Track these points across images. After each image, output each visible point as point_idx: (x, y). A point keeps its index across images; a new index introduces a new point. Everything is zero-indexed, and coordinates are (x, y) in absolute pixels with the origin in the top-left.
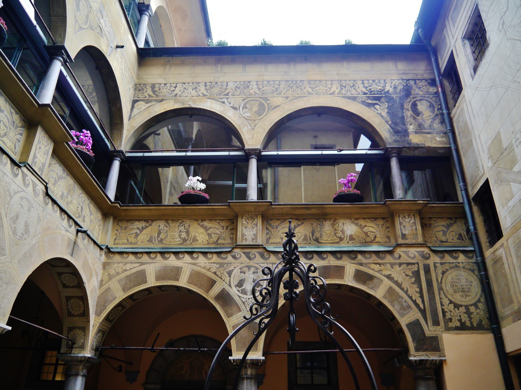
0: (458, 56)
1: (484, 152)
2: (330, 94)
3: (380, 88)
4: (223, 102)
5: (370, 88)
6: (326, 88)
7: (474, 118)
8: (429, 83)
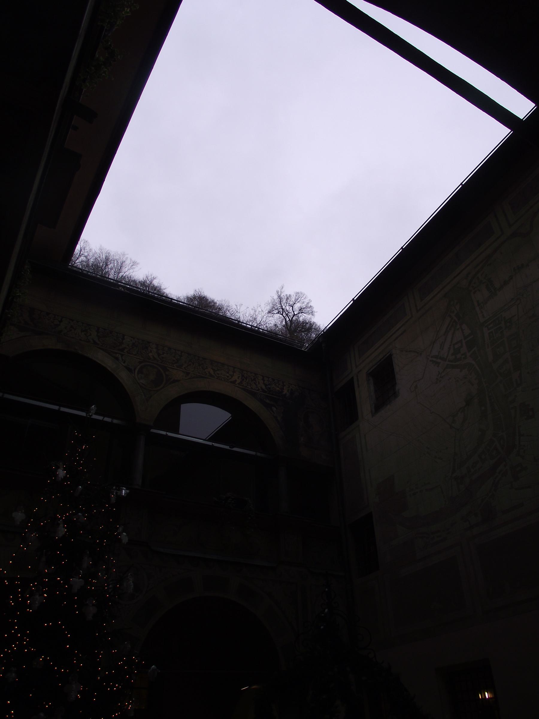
2: (231, 382)
3: (278, 389)
4: (117, 359)
5: (269, 386)
6: (228, 375)
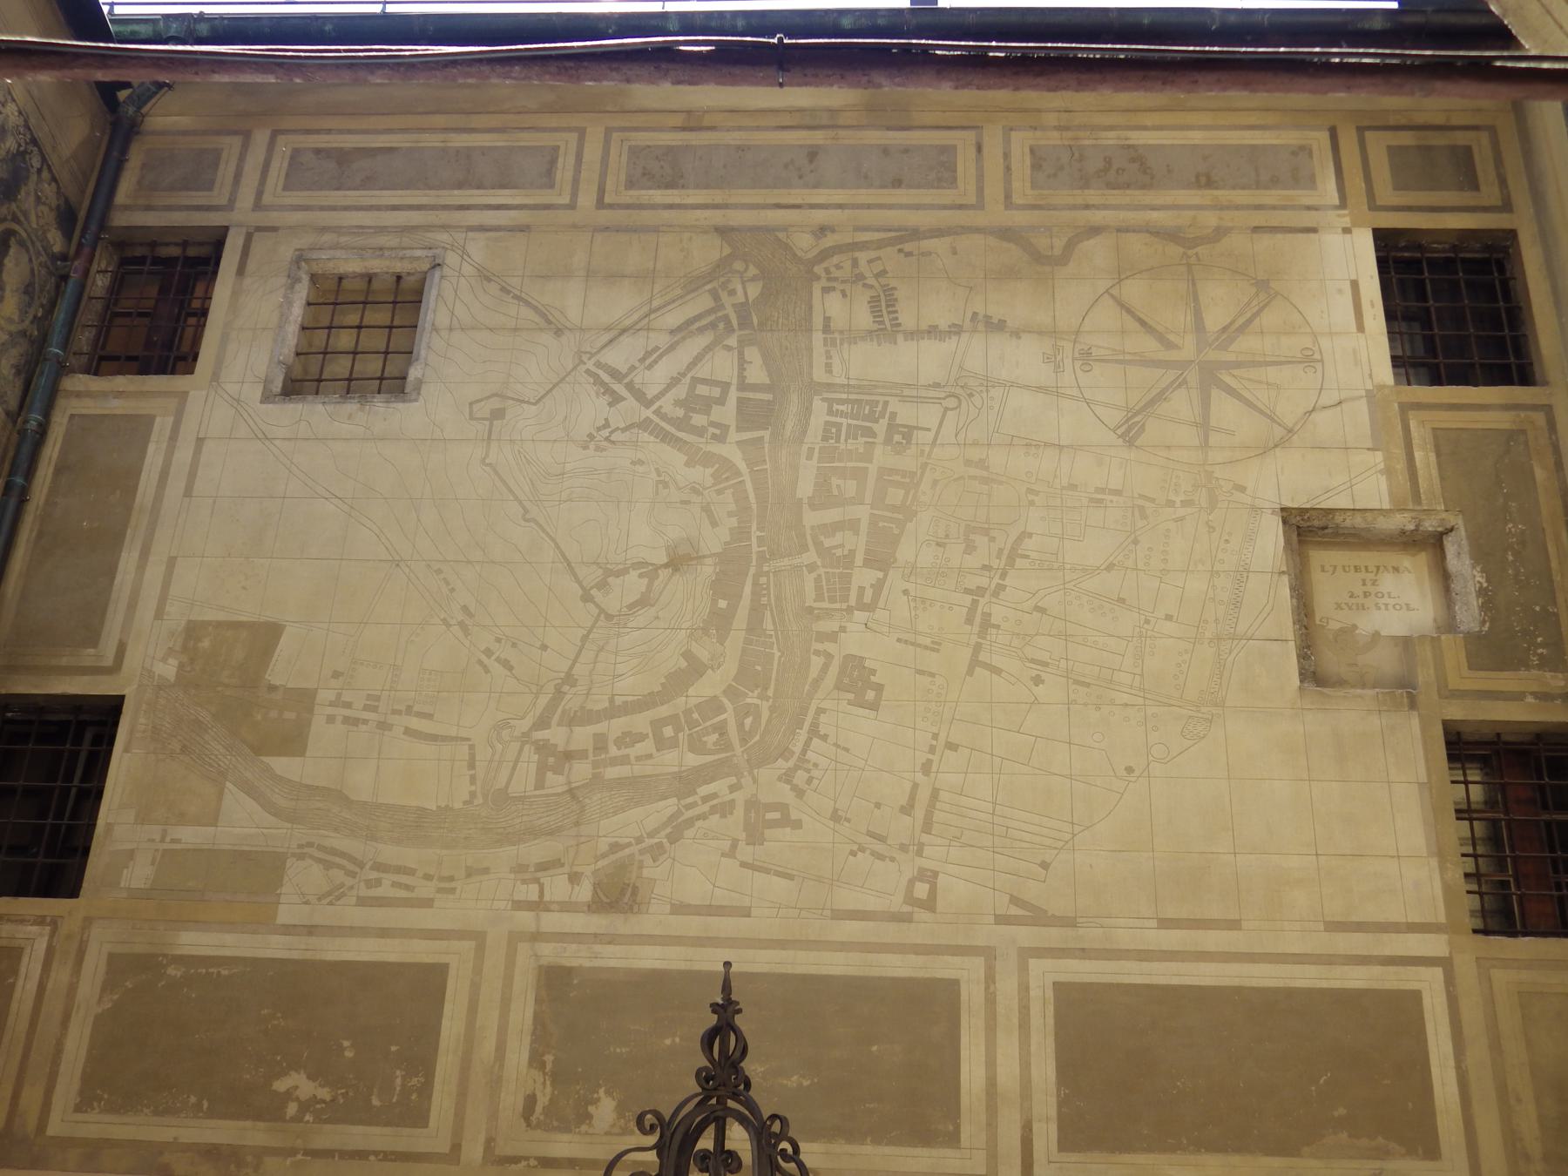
0: (241, 271)
1: (159, 614)
7: (188, 492)
8: (58, 207)
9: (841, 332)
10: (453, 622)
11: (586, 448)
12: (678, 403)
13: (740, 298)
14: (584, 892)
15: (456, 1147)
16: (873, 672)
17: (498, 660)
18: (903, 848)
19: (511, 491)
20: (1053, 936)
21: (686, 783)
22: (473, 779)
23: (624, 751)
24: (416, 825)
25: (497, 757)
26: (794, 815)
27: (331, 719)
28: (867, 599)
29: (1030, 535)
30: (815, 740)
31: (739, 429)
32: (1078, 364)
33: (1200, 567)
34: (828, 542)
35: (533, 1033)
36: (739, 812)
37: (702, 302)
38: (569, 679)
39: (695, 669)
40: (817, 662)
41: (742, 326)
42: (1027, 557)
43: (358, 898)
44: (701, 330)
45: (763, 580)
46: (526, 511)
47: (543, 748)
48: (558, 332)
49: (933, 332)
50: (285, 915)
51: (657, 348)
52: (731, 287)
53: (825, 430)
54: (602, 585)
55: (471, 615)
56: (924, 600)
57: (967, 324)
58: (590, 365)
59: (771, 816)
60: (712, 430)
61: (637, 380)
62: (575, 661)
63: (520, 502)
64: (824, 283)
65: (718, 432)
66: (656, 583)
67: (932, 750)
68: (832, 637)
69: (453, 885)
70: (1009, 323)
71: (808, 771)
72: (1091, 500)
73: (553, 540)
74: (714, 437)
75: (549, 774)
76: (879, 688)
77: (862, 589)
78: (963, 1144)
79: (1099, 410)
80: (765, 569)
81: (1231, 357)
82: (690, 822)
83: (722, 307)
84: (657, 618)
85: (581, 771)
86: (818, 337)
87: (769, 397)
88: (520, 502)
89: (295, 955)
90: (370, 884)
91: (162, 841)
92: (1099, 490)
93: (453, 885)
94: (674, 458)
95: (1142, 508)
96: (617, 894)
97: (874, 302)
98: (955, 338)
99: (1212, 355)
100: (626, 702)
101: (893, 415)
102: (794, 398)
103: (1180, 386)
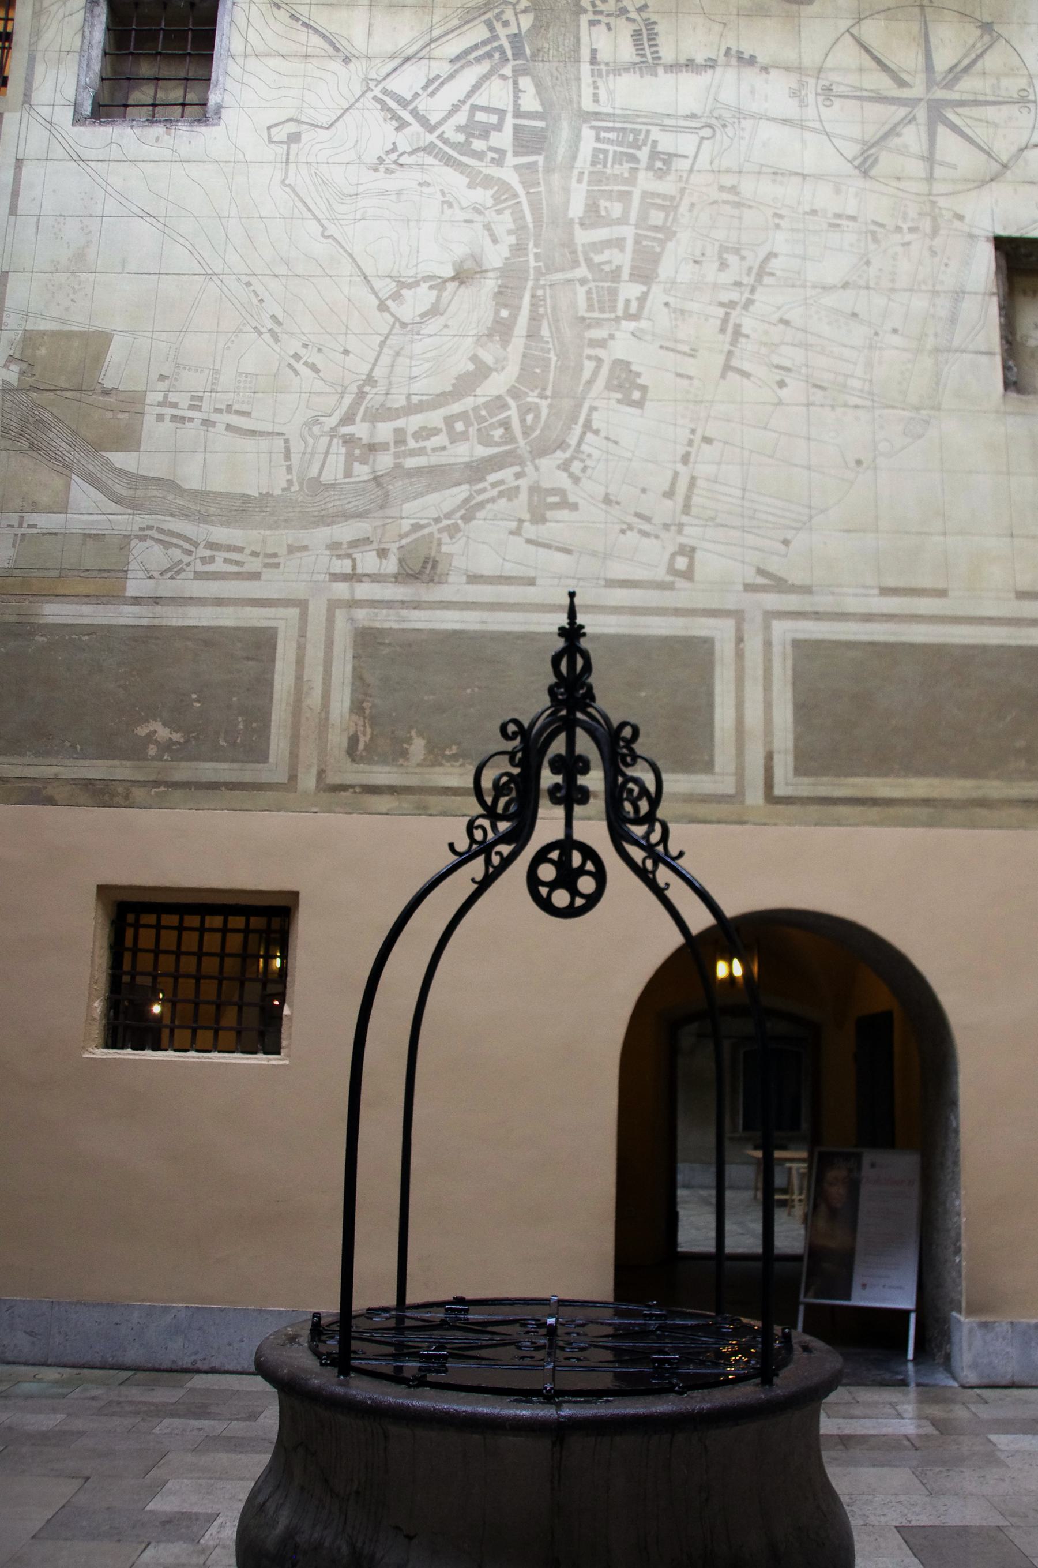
9: (607, 64)
10: (263, 330)
11: (376, 170)
12: (459, 129)
13: (514, 30)
14: (391, 566)
15: (293, 777)
16: (639, 375)
17: (306, 363)
18: (666, 527)
19: (309, 210)
20: (792, 602)
21: (476, 471)
22: (289, 469)
23: (421, 444)
24: (241, 508)
25: (309, 450)
26: (572, 499)
27: (160, 417)
28: (633, 308)
29: (776, 255)
30: (590, 437)
31: (516, 154)
32: (820, 99)
33: (923, 287)
34: (597, 259)
35: (353, 684)
36: (524, 496)
37: (478, 33)
38: (370, 380)
39: (482, 371)
40: (589, 366)
41: (516, 56)
42: (773, 275)
43: (195, 572)
44: (478, 60)
45: (540, 293)
46: (324, 228)
47: (349, 441)
48: (347, 60)
49: (690, 65)
50: (133, 589)
51: (438, 77)
52: (504, 17)
53: (595, 156)
54: (396, 296)
55: (279, 324)
56: (682, 312)
57: (722, 59)
58: (377, 92)
59: (551, 499)
60: (491, 155)
61: (421, 107)
62: (374, 365)
63: (319, 220)
64: (590, 16)
65: (496, 156)
66: (445, 294)
67: (690, 443)
68: (602, 344)
69: (276, 560)
70: (759, 59)
71: (583, 461)
72: (830, 225)
73: (351, 256)
74: (493, 159)
75: (356, 464)
76: (644, 389)
77: (628, 302)
78: (717, 768)
79: (838, 143)
80: (542, 282)
81: (956, 96)
82: (481, 505)
83: (495, 37)
84: (446, 326)
85: (385, 461)
86: (585, 68)
87: (541, 124)
88: (319, 220)
89: (145, 622)
90: (204, 560)
91: (20, 526)
92: (838, 216)
93: (276, 560)
94: (455, 180)
95: (873, 233)
96: (421, 568)
97: (637, 35)
98: (710, 72)
99: (940, 94)
100: (421, 401)
101: (655, 142)
102: (565, 124)
103: (910, 122)
